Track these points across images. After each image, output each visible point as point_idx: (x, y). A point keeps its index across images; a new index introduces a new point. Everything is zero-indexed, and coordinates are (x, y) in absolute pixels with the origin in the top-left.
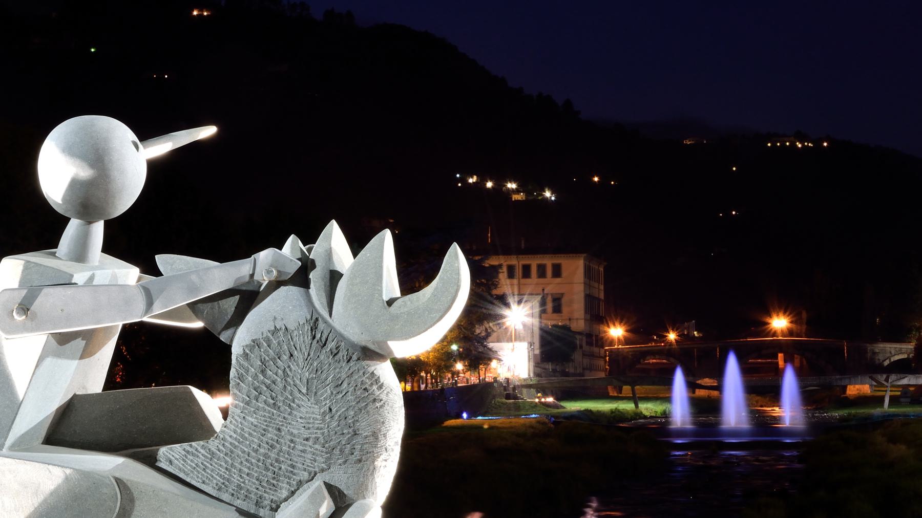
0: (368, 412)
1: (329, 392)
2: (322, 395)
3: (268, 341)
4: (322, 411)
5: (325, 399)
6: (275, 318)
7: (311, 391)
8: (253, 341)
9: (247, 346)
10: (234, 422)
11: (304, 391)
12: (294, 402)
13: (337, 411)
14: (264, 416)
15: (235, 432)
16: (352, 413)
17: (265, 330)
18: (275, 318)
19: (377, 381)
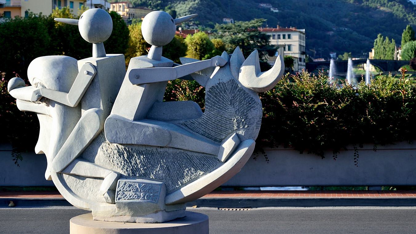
0: (251, 111)
1: (238, 104)
2: (235, 105)
3: (217, 86)
4: (235, 110)
5: (237, 106)
6: (219, 79)
7: (232, 104)
8: (212, 87)
9: (210, 88)
10: (206, 113)
11: (230, 103)
12: (226, 107)
13: (240, 110)
14: (217, 112)
15: (207, 116)
16: (246, 111)
17: (216, 83)
18: (219, 79)
19: (70, 146)
